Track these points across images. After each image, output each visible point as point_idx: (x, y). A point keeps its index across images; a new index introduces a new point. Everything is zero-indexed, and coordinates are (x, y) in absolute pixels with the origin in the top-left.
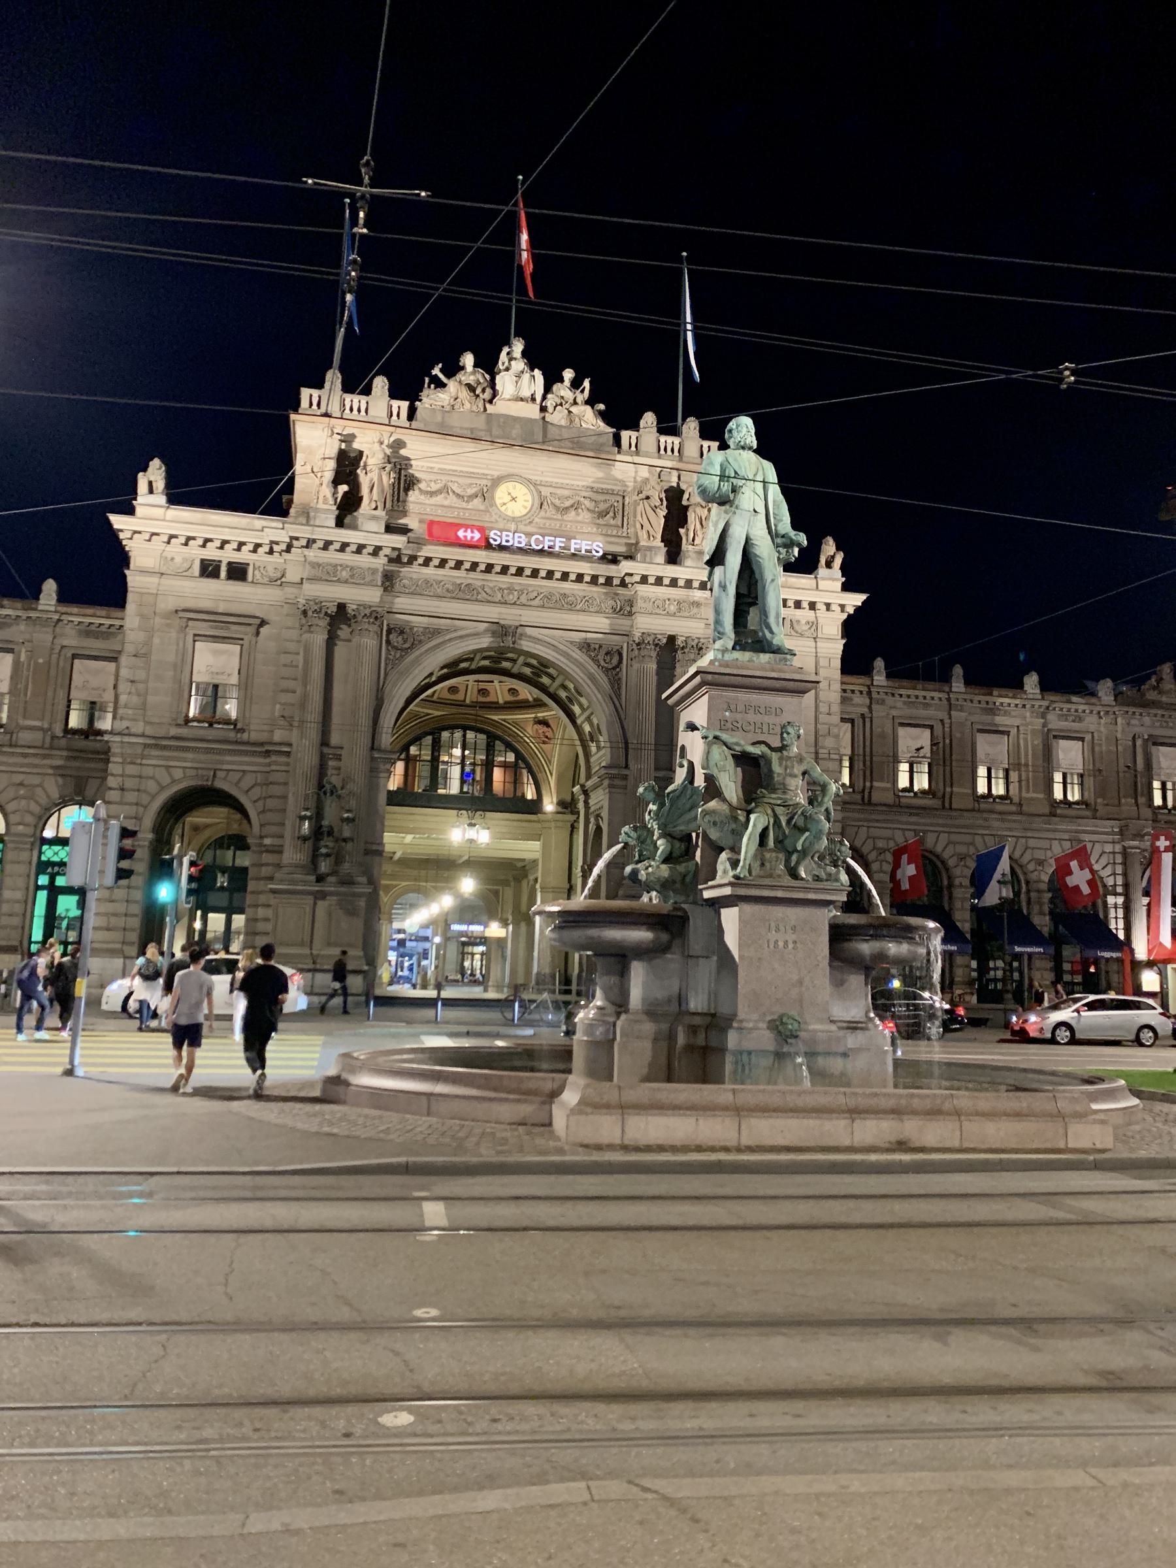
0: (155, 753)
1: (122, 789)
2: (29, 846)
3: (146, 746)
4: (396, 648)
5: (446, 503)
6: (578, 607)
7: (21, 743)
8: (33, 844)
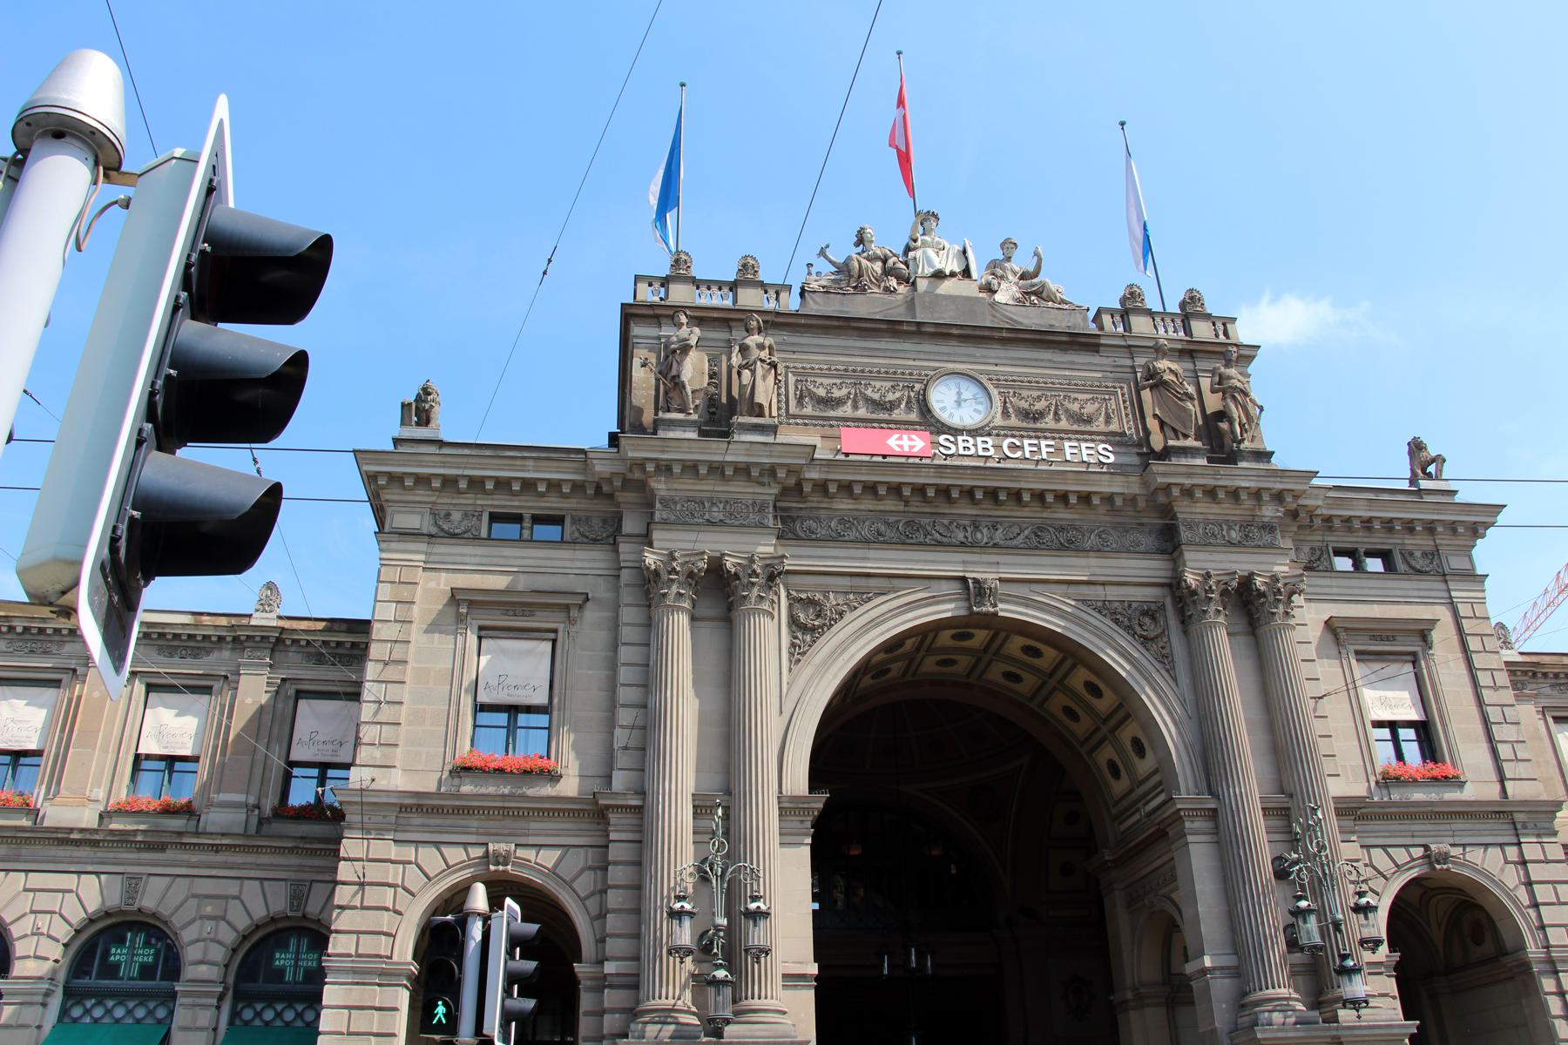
0: (417, 820)
1: (362, 885)
2: (214, 1001)
3: (403, 808)
4: (804, 628)
5: (862, 412)
6: (1088, 545)
7: (209, 829)
8: (221, 997)
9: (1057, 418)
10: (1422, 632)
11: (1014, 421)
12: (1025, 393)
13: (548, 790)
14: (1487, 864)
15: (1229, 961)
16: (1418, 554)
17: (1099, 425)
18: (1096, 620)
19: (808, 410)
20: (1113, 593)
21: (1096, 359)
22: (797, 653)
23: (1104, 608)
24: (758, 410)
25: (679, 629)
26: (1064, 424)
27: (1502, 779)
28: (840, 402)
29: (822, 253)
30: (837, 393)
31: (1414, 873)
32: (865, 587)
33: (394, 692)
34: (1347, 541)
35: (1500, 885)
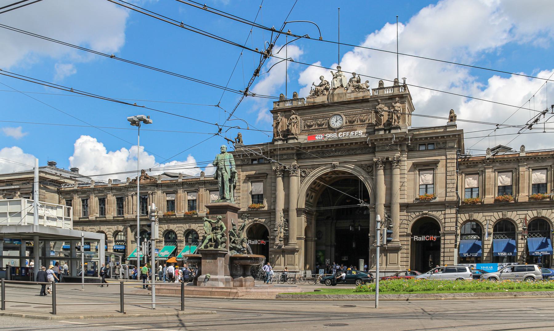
5: (317, 127)
9: (357, 122)
10: (436, 163)
11: (348, 124)
12: (351, 116)
13: (263, 209)
14: (437, 215)
15: (373, 235)
16: (441, 143)
17: (367, 122)
18: (358, 169)
19: (306, 128)
20: (363, 163)
21: (368, 104)
22: (302, 182)
23: (361, 166)
24: (293, 135)
25: (280, 180)
26: (359, 123)
27: (446, 196)
28: (312, 126)
29: (313, 84)
30: (312, 123)
31: (420, 217)
32: (314, 167)
33: (239, 194)
34: (421, 142)
35: (439, 219)
